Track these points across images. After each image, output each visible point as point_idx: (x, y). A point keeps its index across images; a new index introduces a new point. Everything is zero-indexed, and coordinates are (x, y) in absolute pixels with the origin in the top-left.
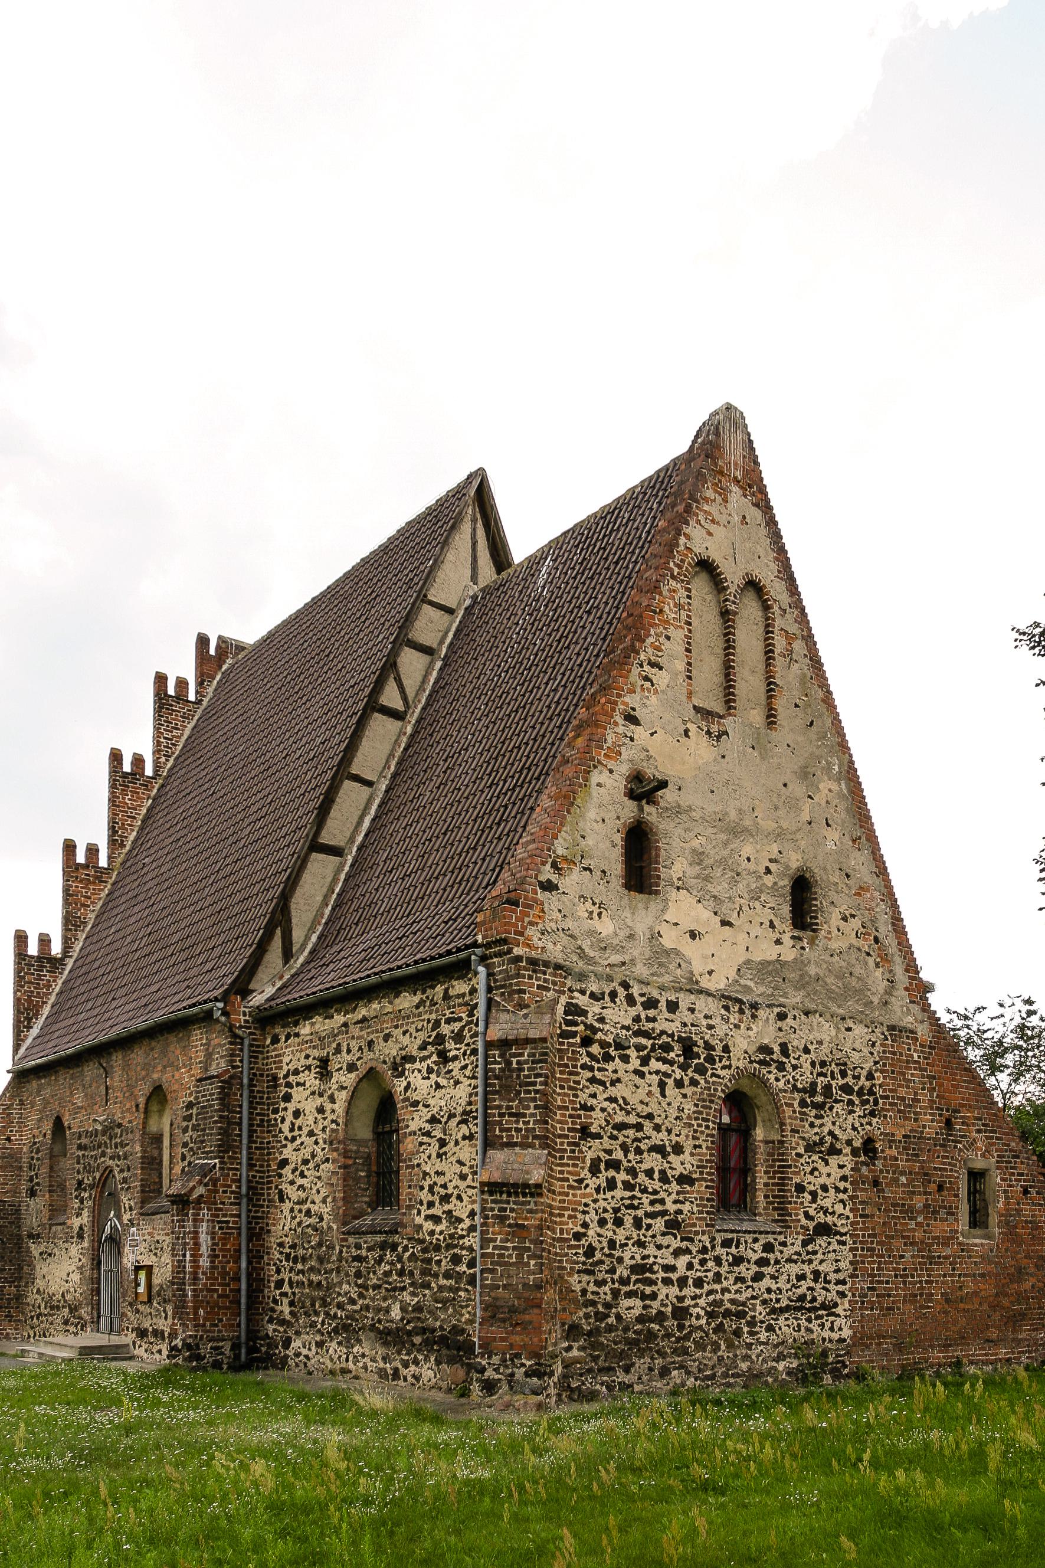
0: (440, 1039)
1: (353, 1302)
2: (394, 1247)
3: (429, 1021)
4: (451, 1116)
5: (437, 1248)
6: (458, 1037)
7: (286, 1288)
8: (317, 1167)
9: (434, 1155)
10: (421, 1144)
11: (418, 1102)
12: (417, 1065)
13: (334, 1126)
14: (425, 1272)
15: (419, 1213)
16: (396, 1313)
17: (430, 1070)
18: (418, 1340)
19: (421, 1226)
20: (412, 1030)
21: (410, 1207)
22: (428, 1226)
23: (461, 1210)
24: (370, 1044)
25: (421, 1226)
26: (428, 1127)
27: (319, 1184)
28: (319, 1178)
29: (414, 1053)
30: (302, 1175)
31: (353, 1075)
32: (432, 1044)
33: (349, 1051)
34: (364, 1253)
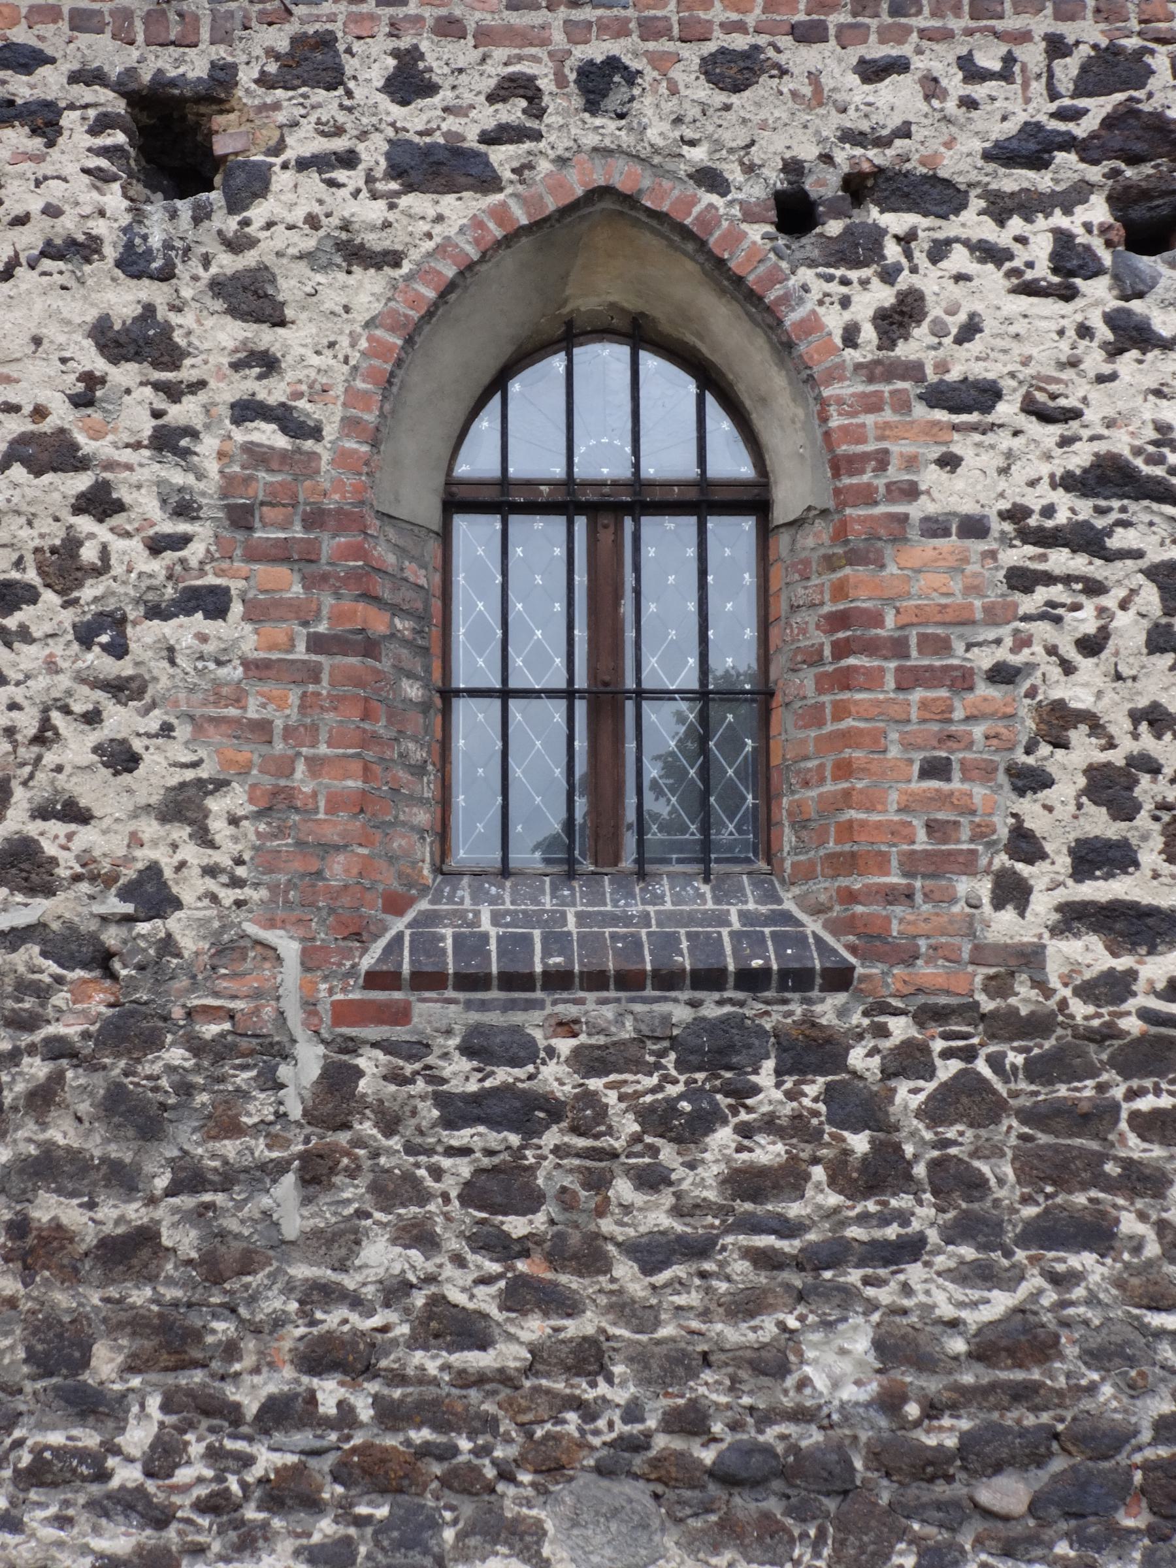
1: (469, 1331)
2: (812, 1052)
3: (1057, 47)
8: (104, 629)
9: (1130, 630)
10: (1023, 580)
11: (986, 395)
12: (973, 223)
13: (267, 434)
14: (1039, 1170)
15: (1011, 892)
16: (838, 1367)
17: (1071, 262)
18: (1007, 1493)
19: (1029, 958)
20: (938, 61)
21: (938, 866)
22: (1090, 953)
24: (599, 84)
25: (1029, 958)
26: (1069, 509)
27: (120, 720)
28: (119, 689)
29: (960, 160)
31: (458, 210)
32: (1088, 150)
33: (409, 82)
34: (555, 1078)
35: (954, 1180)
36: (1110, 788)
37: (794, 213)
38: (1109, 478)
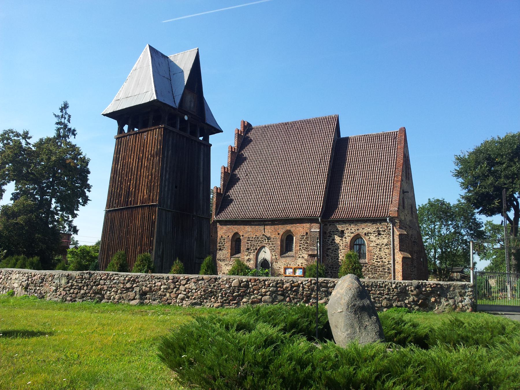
0: (379, 231)
2: (366, 266)
4: (383, 244)
5: (379, 267)
6: (384, 231)
7: (330, 273)
23: (386, 261)
30: (335, 252)
33: (351, 230)
35: (371, 271)
36: (377, 257)
37: (365, 234)
38: (377, 244)
